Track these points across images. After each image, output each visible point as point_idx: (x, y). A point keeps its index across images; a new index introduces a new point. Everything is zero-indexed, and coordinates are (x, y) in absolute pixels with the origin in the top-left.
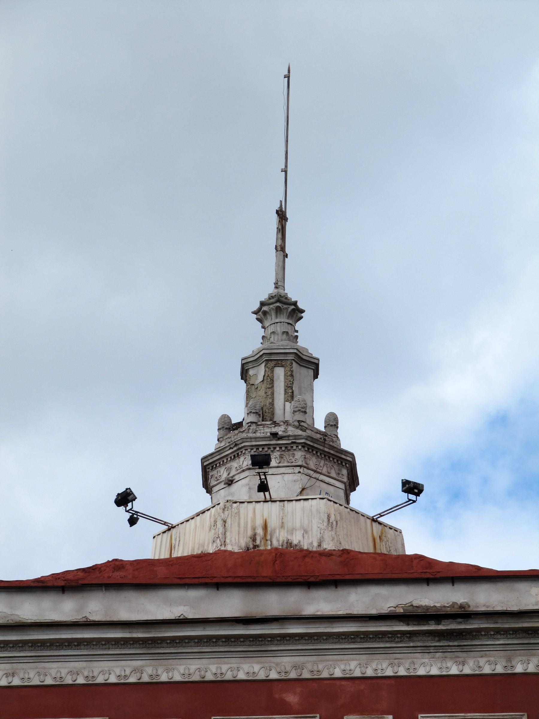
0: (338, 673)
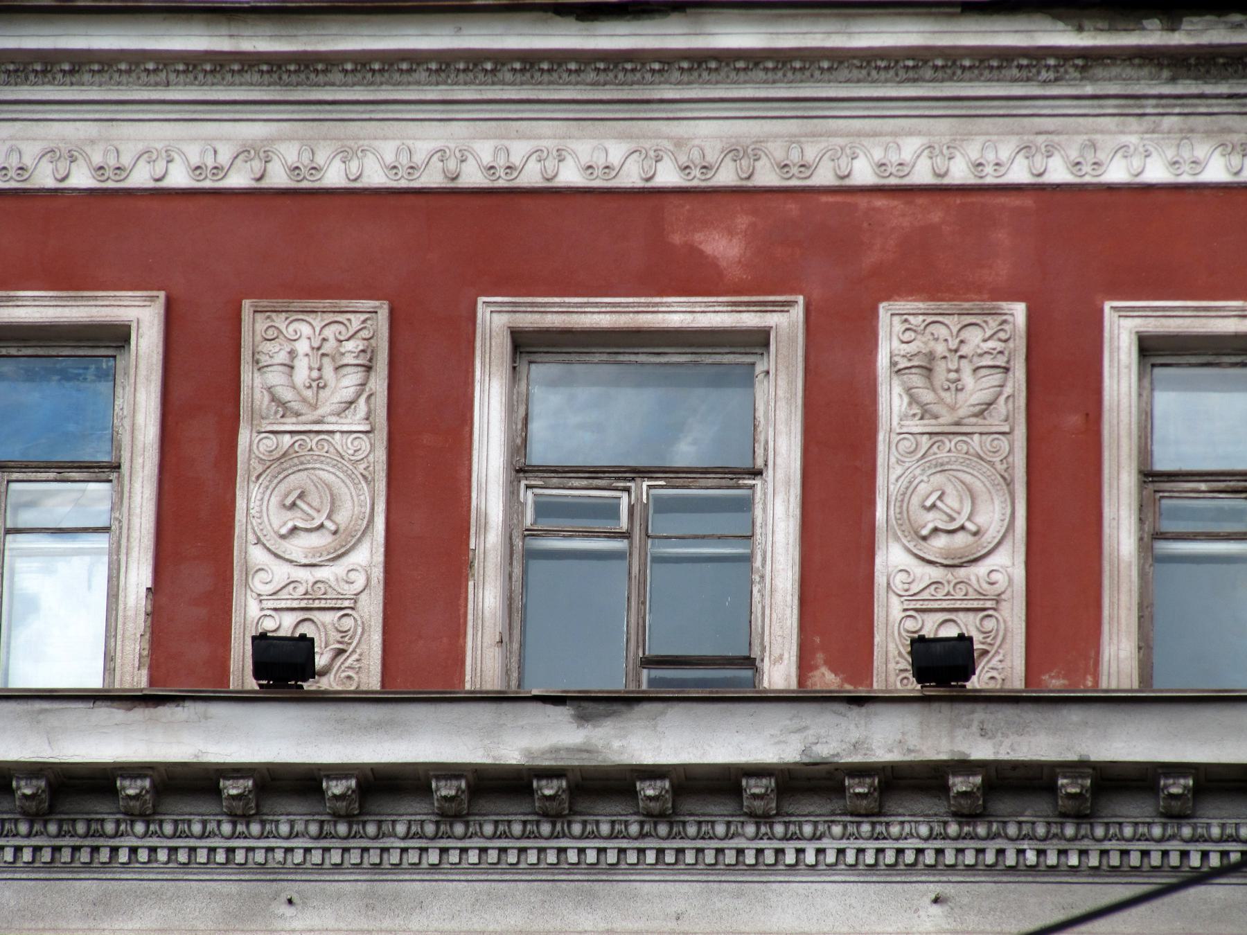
0: (863, 174)
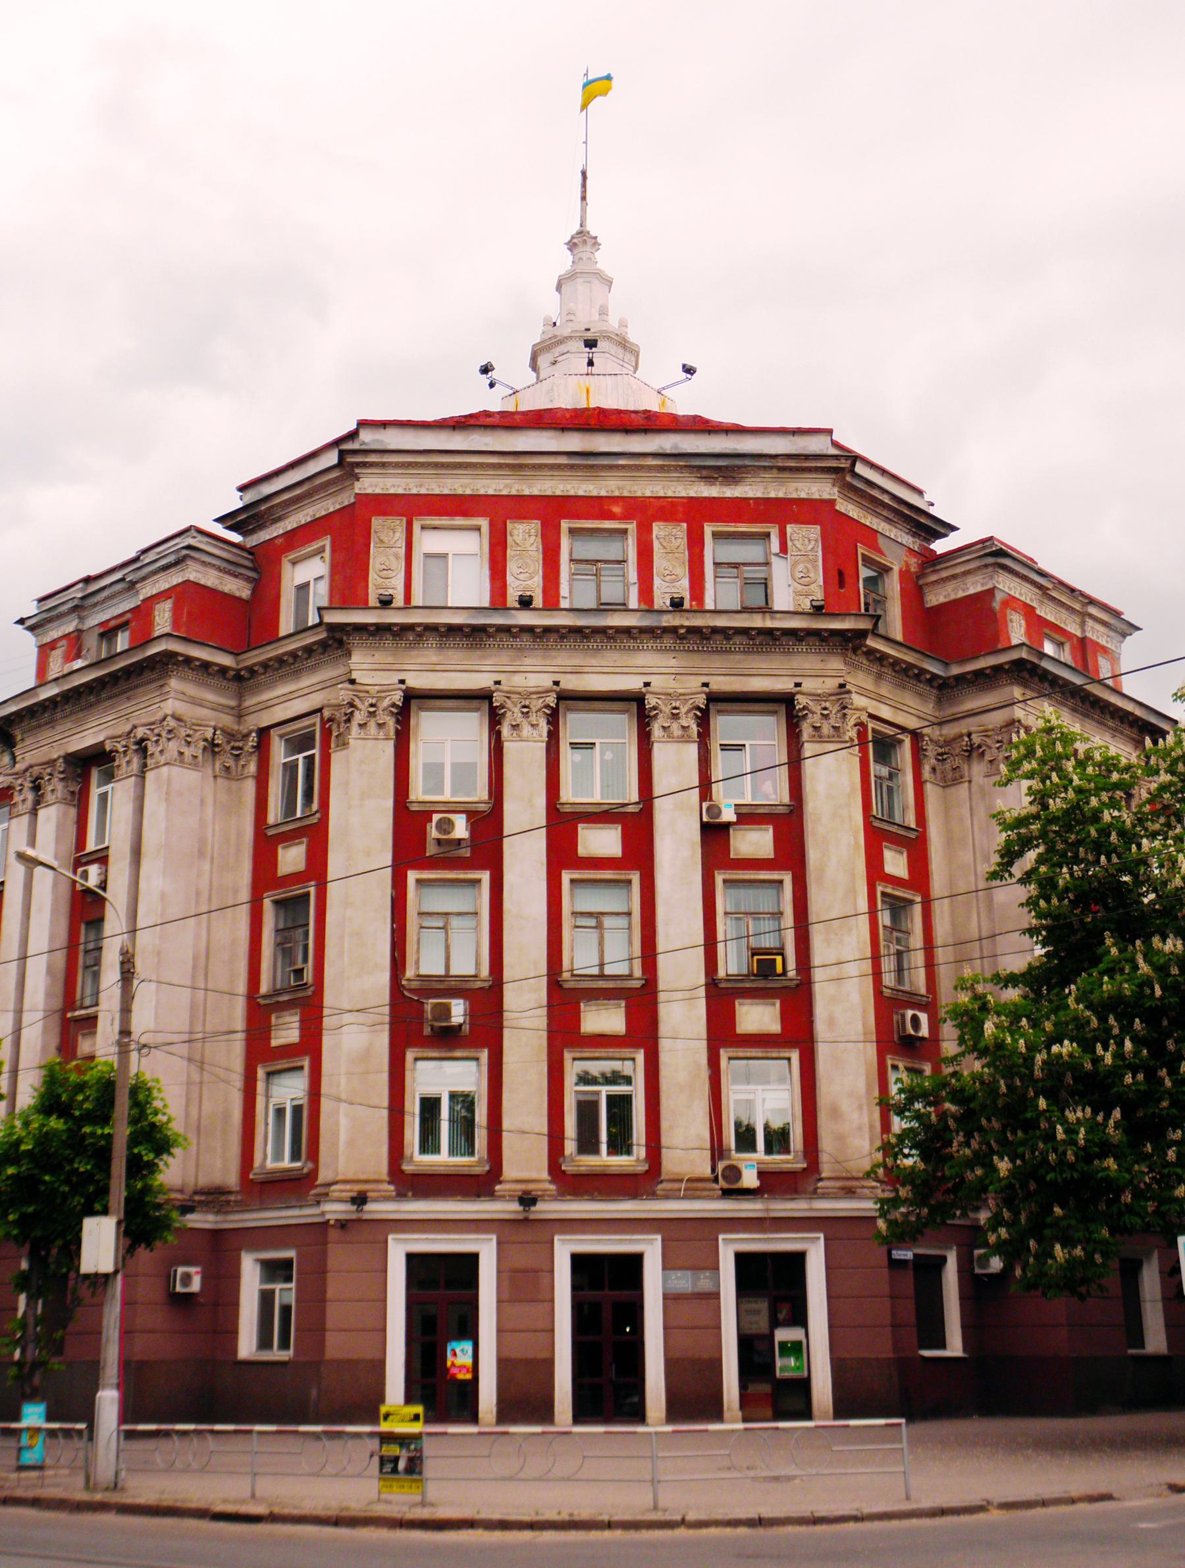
0: (648, 494)
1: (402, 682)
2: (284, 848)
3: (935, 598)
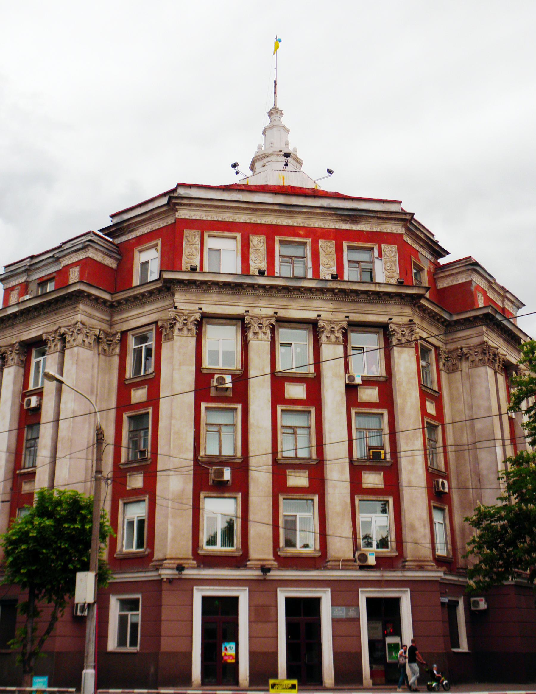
0: (316, 226)
1: (200, 309)
2: (135, 390)
3: (442, 284)
